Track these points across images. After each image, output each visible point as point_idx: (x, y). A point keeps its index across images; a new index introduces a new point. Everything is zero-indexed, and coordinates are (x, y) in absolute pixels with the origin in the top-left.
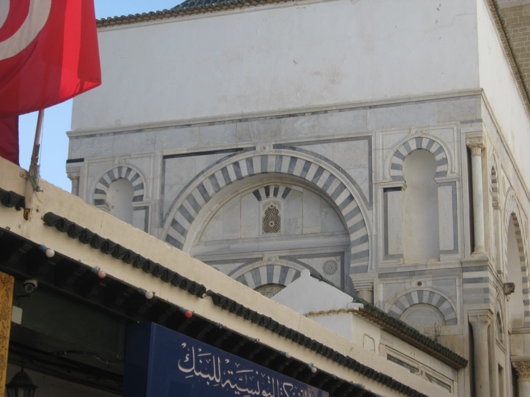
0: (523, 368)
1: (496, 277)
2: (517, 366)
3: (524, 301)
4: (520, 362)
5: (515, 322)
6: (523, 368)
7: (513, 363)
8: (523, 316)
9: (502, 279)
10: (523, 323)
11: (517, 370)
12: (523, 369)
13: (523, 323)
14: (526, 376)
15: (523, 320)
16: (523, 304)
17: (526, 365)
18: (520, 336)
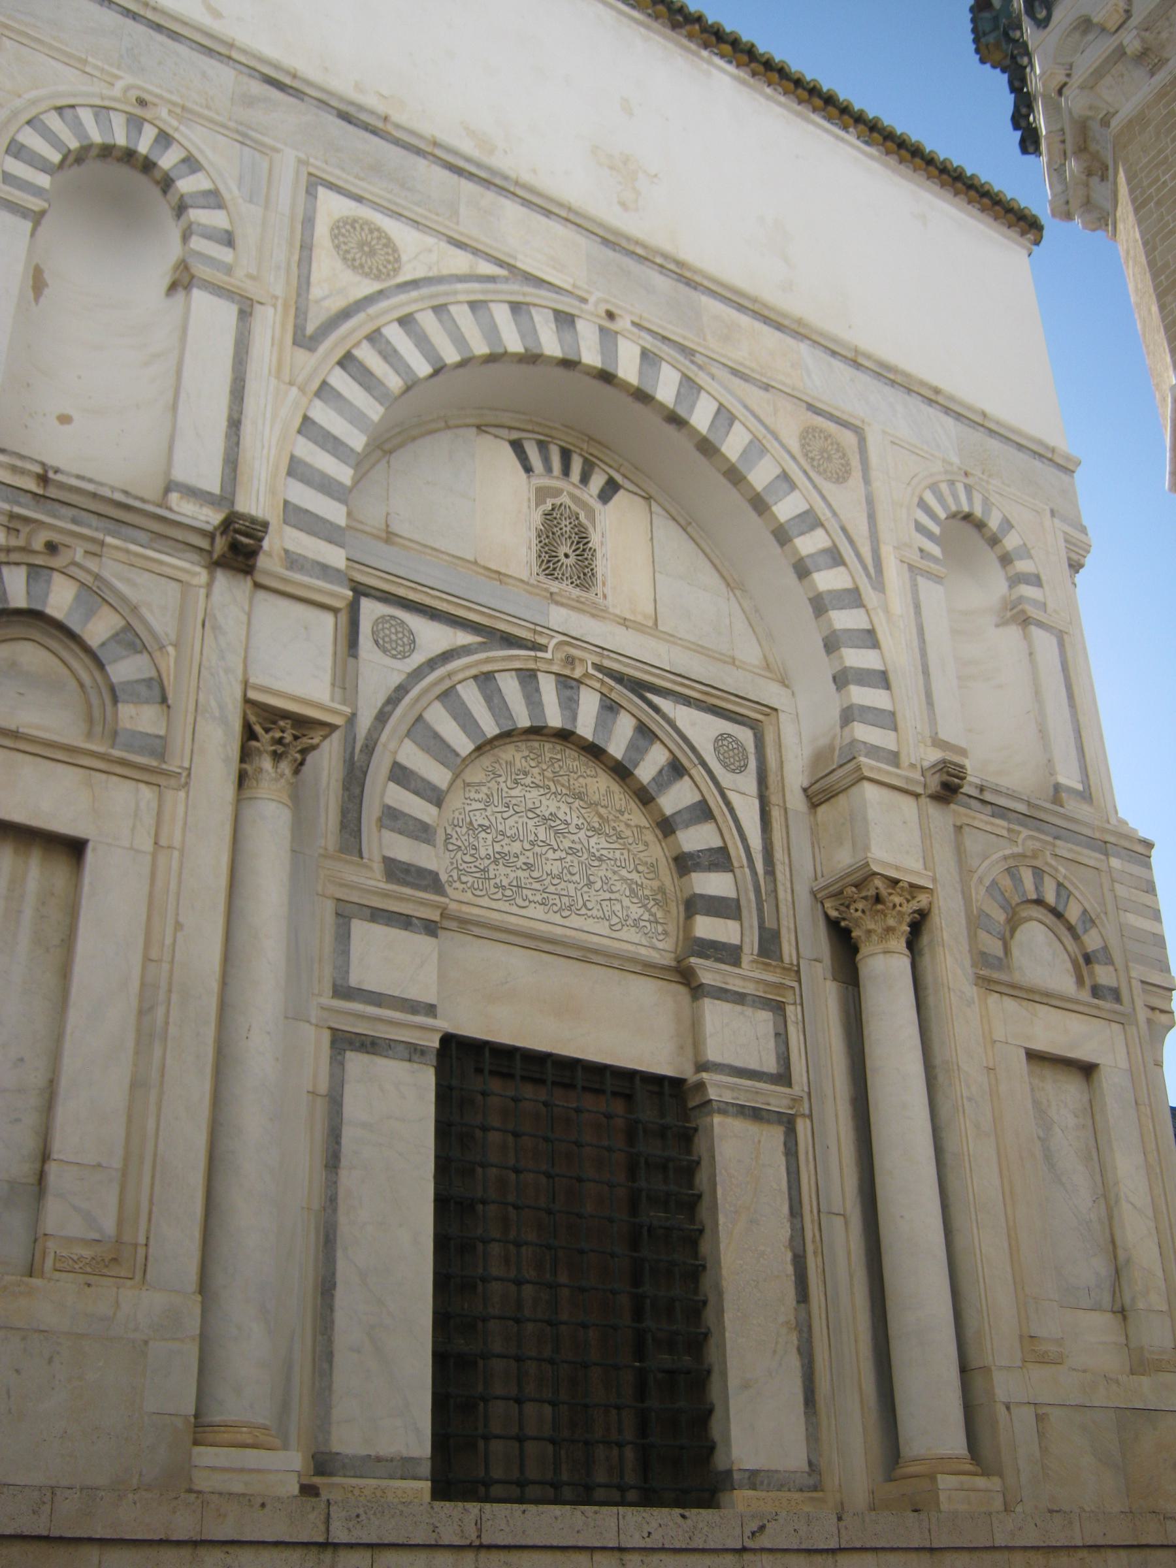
0: (856, 910)
1: (32, 485)
2: (842, 908)
3: (834, 678)
4: (841, 892)
5: (819, 758)
6: (856, 910)
7: (827, 905)
8: (838, 729)
9: (170, 509)
10: (837, 753)
11: (843, 924)
12: (859, 914)
13: (837, 753)
14: (875, 938)
15: (837, 742)
16: (833, 687)
17: (865, 898)
18: (842, 800)
